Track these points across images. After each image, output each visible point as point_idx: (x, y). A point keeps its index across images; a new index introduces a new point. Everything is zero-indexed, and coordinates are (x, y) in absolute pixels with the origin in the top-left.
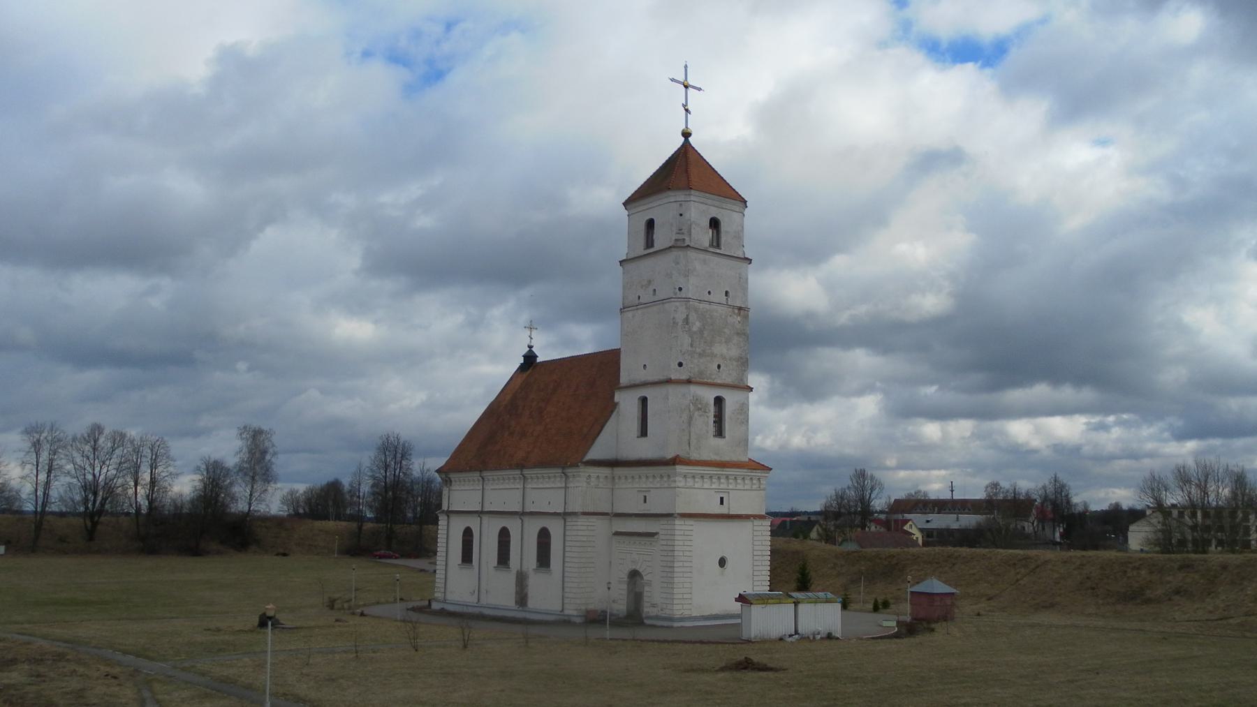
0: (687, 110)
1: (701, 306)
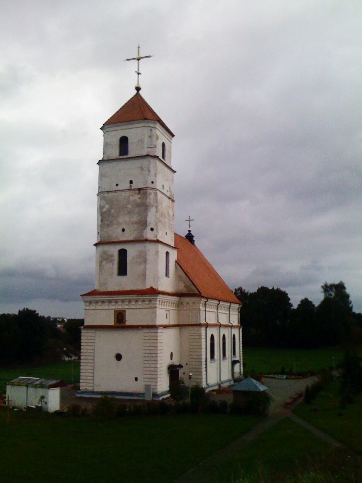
0: (138, 74)
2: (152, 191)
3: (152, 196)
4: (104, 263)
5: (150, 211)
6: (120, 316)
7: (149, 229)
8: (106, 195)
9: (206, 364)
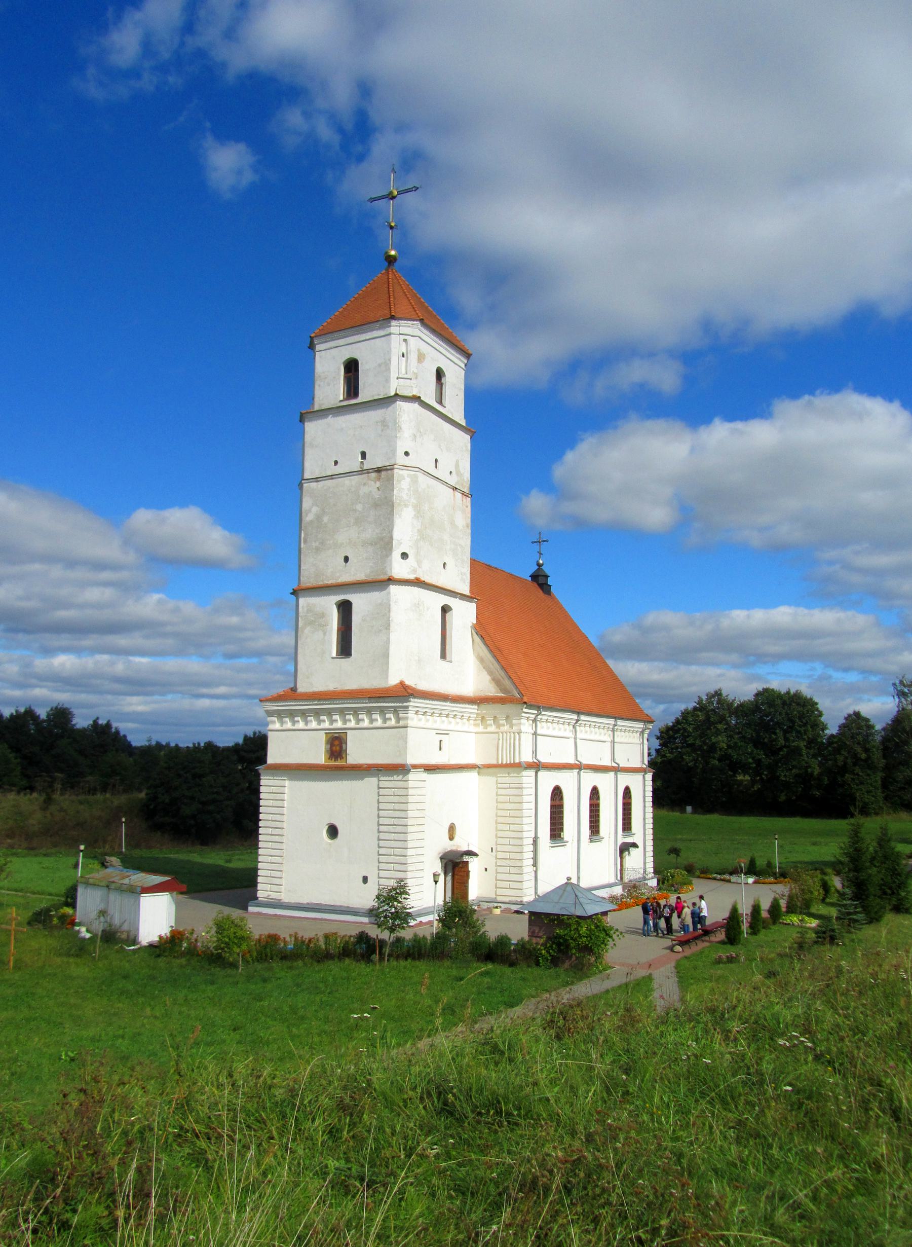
1: (321, 484)
4: (307, 630)
6: (336, 745)
7: (396, 555)
8: (314, 485)
9: (535, 851)
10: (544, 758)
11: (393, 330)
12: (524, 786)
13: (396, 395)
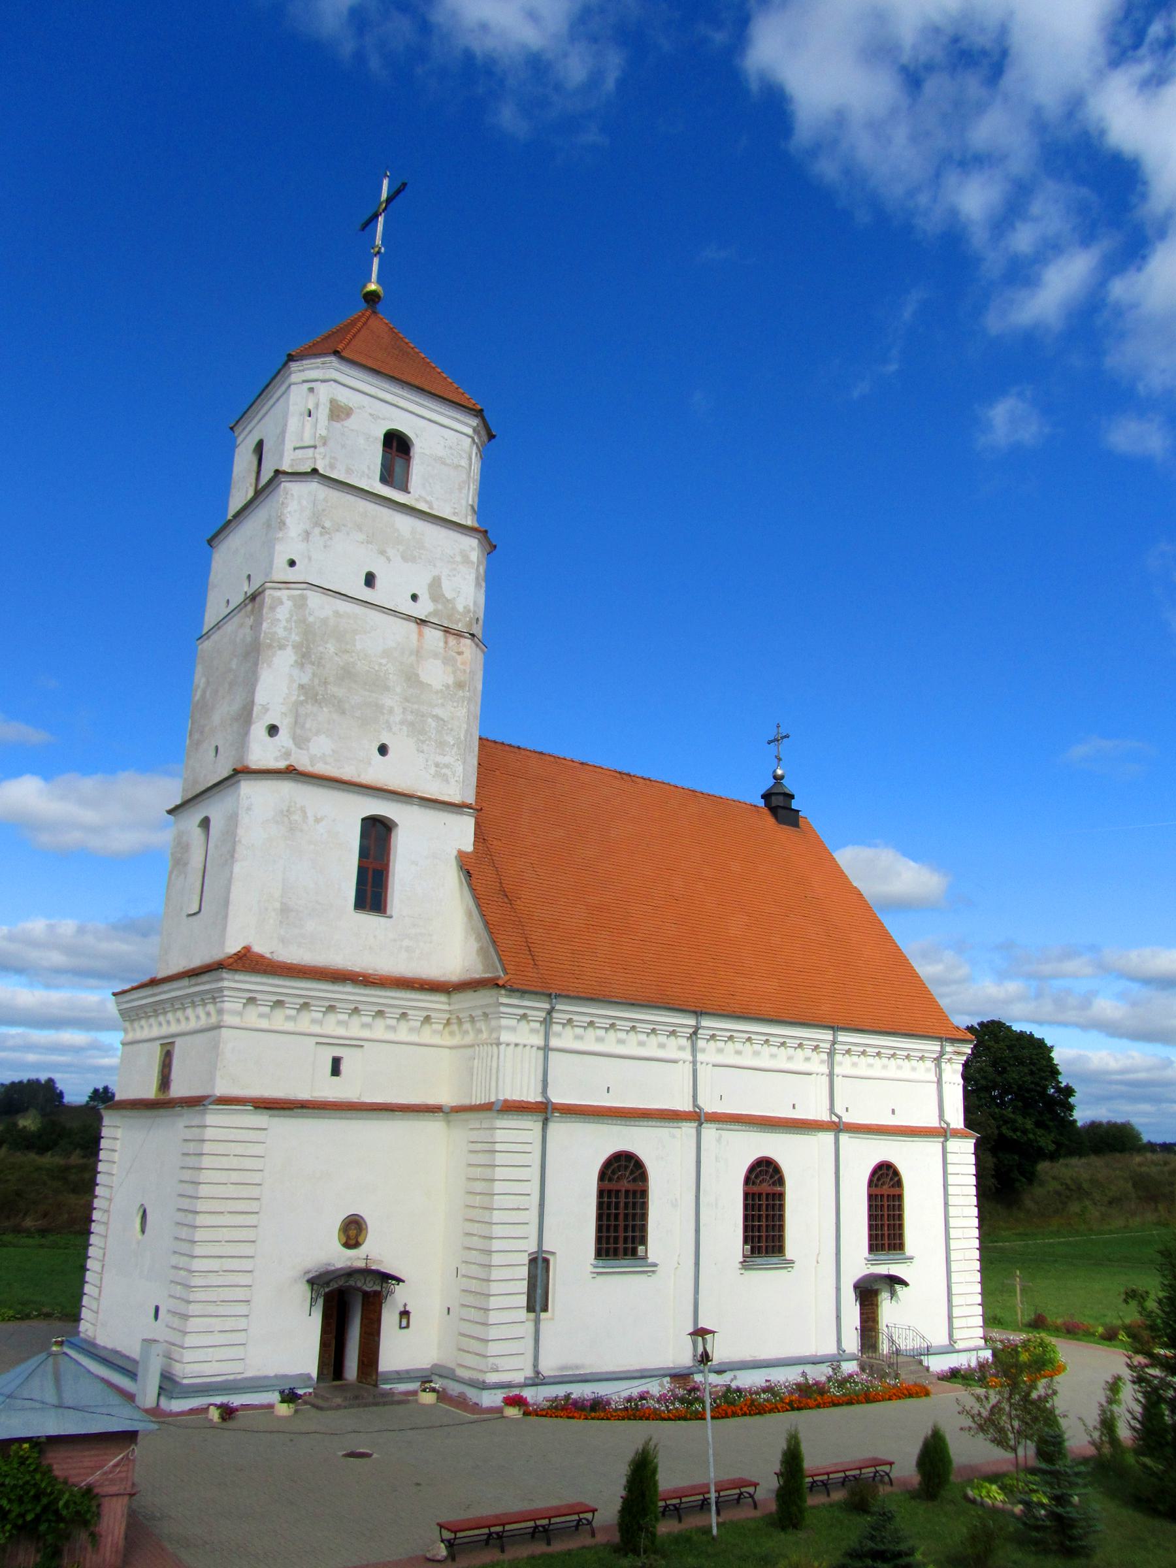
2: (284, 594)
3: (283, 612)
5: (269, 666)
7: (258, 731)
10: (709, 1105)
11: (295, 378)
12: (498, 1147)
13: (277, 472)
